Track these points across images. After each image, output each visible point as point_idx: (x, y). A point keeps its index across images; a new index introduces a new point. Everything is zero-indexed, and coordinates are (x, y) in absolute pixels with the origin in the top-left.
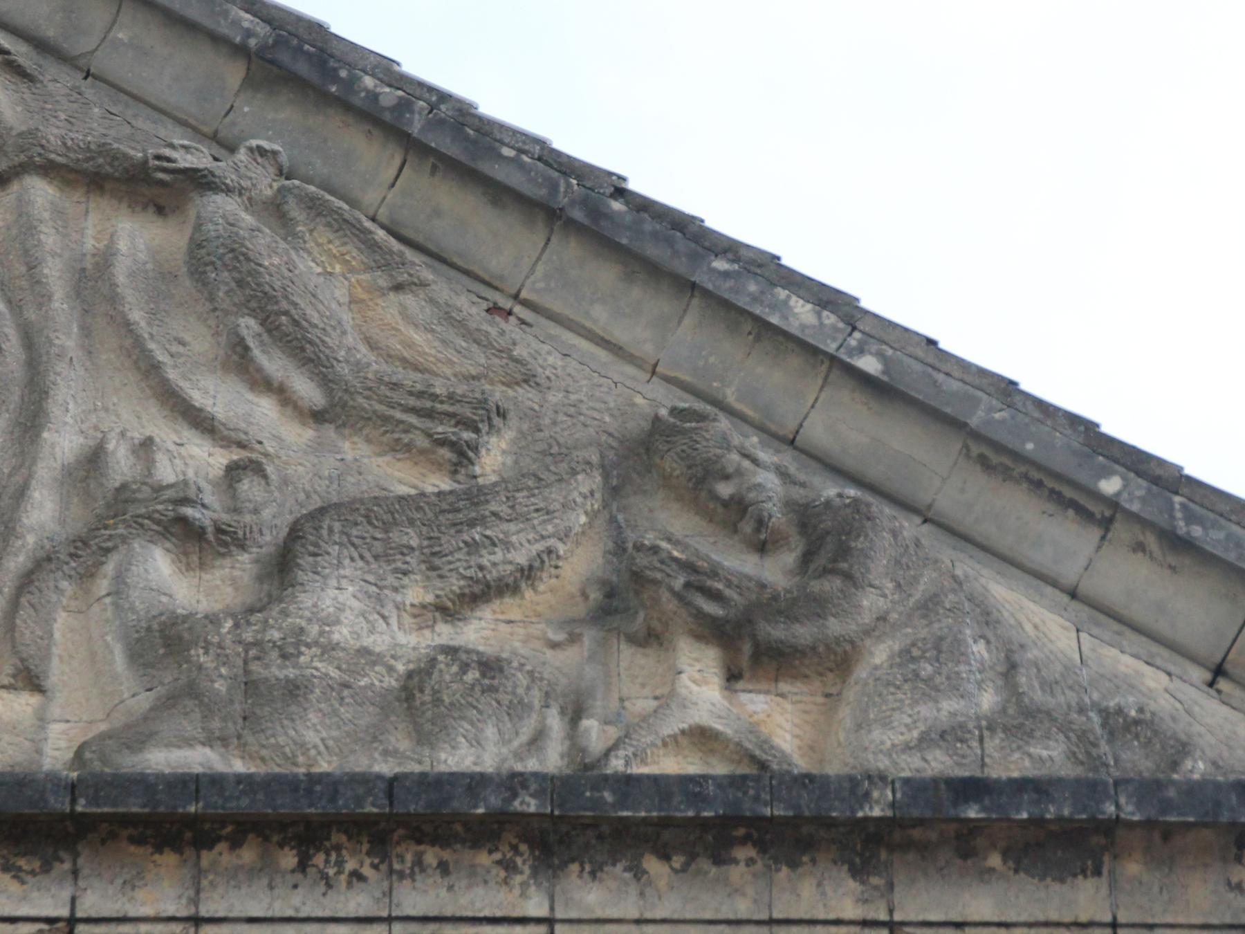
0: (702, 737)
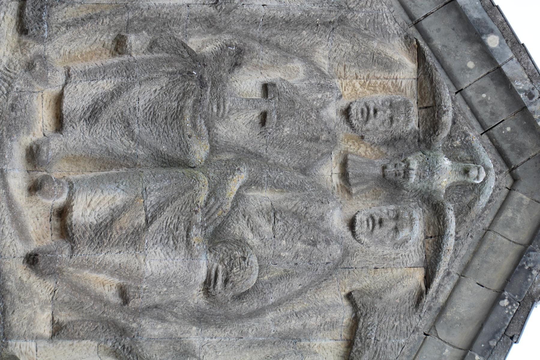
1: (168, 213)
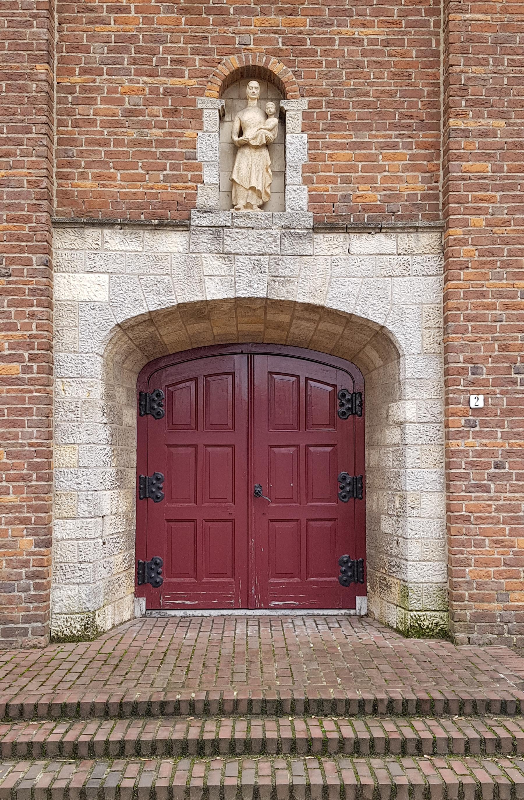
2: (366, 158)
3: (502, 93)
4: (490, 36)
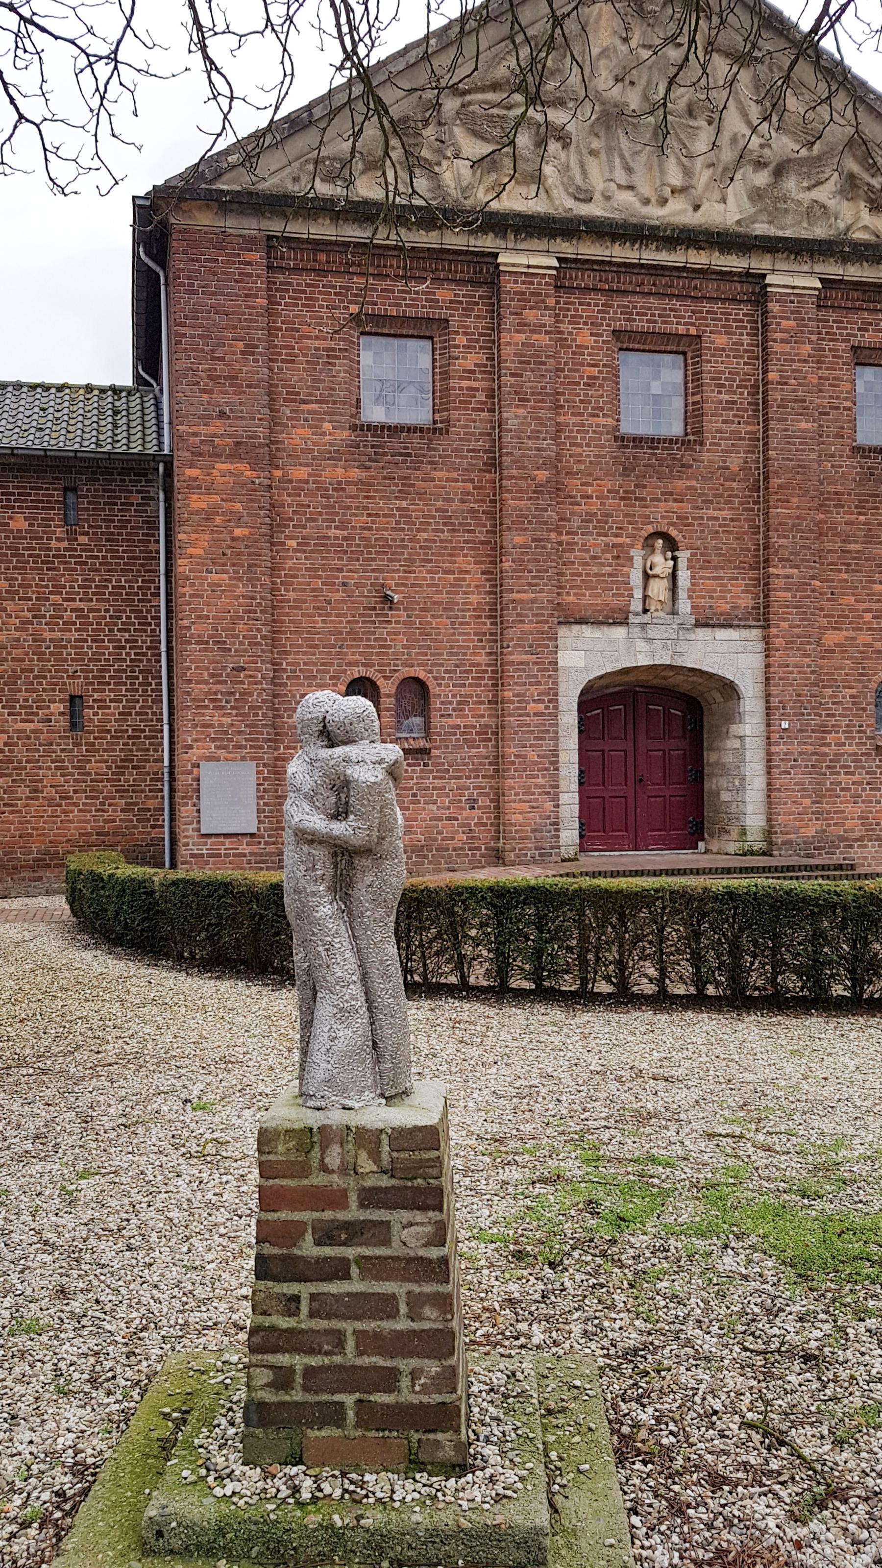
0: (865, 228)
1: (682, 136)
2: (721, 585)
3: (797, 554)
4: (790, 522)
